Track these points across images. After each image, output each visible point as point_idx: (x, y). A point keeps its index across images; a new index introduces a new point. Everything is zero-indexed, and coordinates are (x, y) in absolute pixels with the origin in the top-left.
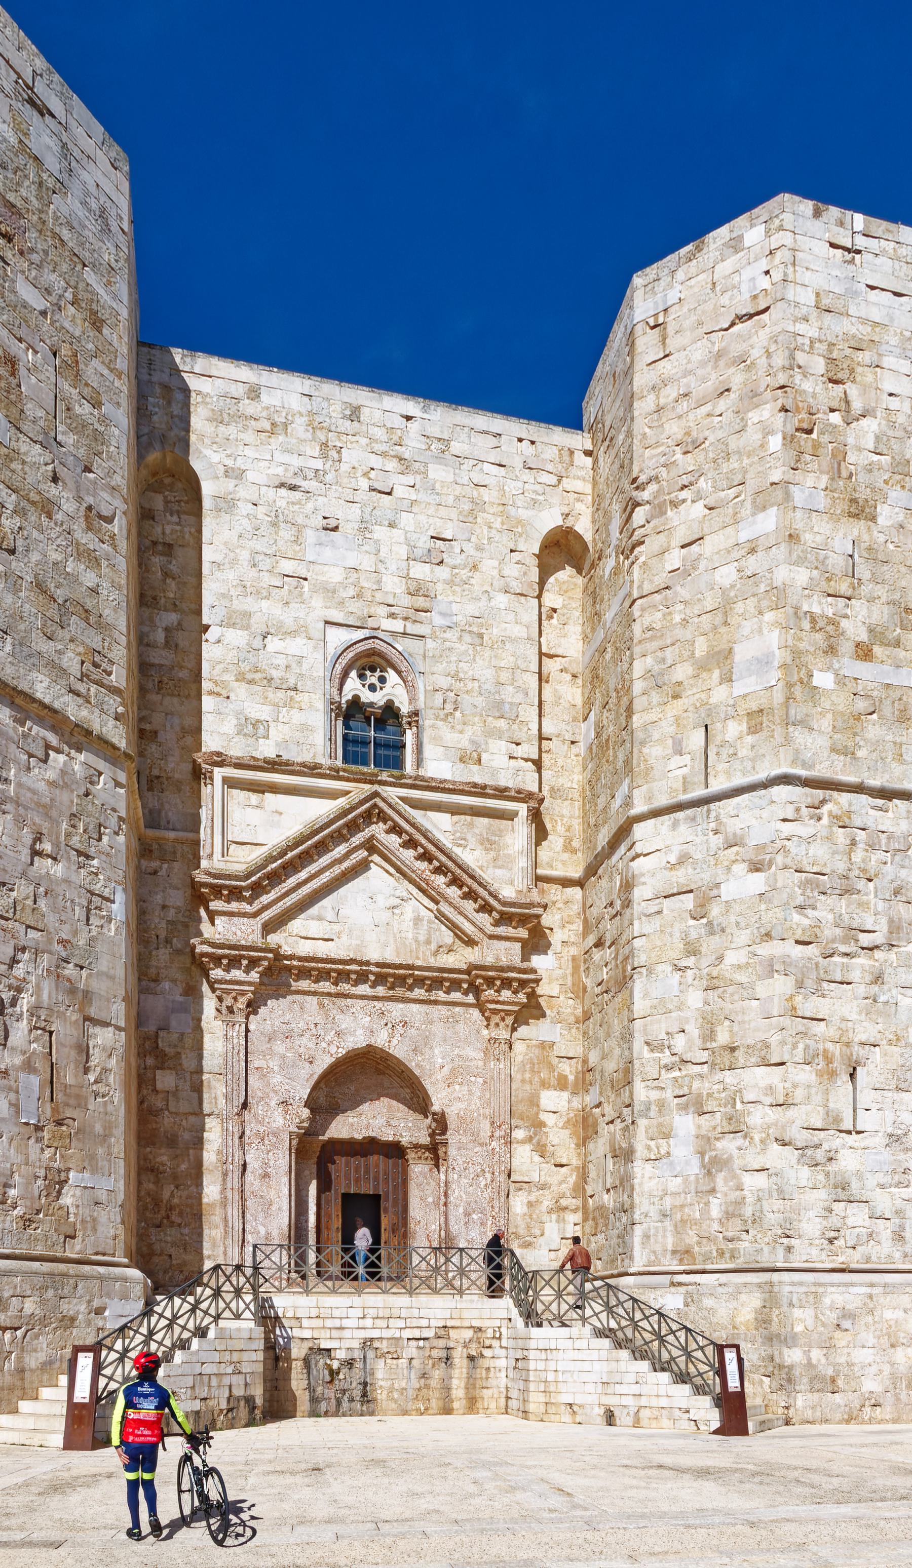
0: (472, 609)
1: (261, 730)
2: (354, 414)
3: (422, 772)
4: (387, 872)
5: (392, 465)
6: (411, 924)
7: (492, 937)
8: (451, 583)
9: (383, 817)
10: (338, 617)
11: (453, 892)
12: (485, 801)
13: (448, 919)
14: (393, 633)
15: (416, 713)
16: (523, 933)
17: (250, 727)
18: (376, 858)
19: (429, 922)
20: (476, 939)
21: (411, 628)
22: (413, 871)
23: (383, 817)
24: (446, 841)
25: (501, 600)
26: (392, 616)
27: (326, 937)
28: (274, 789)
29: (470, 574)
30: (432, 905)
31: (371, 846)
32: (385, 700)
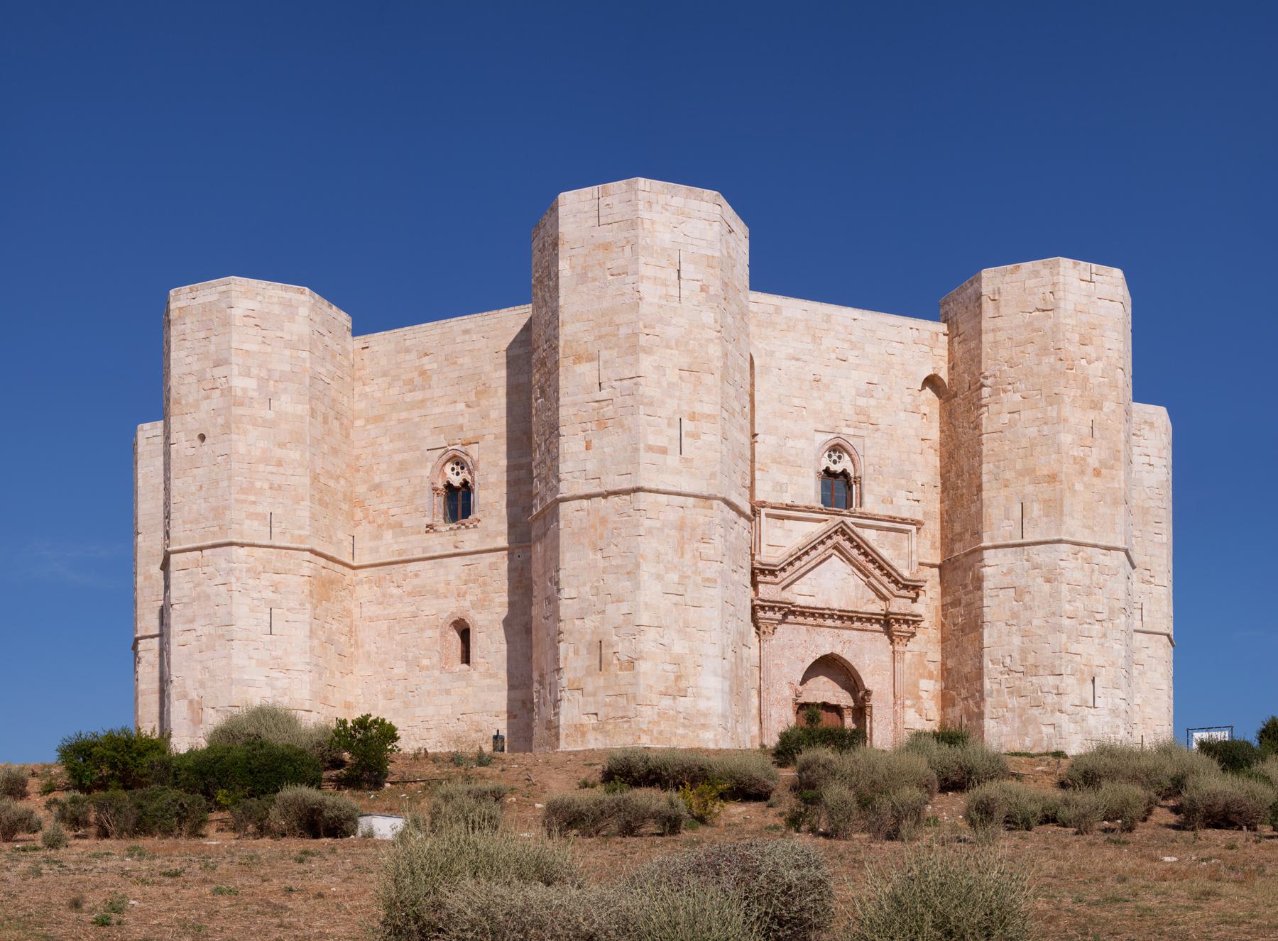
2: (828, 319)
3: (862, 510)
5: (846, 345)
12: (898, 525)
16: (912, 594)
21: (858, 432)
23: (844, 533)
24: (874, 545)
25: (902, 415)
26: (848, 426)
28: (789, 518)
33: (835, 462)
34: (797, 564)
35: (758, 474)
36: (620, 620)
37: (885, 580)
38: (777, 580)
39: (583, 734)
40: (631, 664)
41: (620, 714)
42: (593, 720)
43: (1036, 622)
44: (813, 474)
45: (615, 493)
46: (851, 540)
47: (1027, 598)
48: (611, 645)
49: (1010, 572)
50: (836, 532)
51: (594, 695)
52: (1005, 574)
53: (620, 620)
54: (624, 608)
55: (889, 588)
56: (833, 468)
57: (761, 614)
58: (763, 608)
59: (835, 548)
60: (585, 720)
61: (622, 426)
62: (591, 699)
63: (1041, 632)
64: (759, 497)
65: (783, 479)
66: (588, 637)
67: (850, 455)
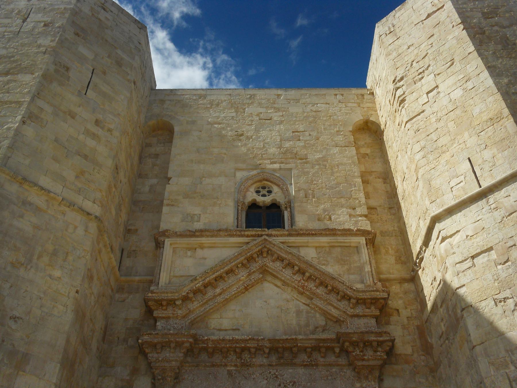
0: (318, 156)
1: (196, 218)
4: (276, 285)
6: (294, 315)
7: (353, 316)
8: (304, 147)
9: (269, 252)
10: (241, 166)
11: (321, 291)
13: (320, 308)
14: (274, 170)
15: (289, 202)
17: (189, 218)
18: (269, 278)
19: (308, 312)
20: (342, 319)
22: (293, 282)
27: (234, 328)
28: (202, 247)
29: (316, 142)
30: (308, 302)
31: (264, 271)
32: (271, 199)
33: (264, 195)
34: (210, 293)
35: (165, 209)
37: (333, 298)
38: (180, 312)
44: (231, 203)
46: (281, 259)
50: (260, 253)
55: (337, 308)
56: (260, 199)
57: (153, 356)
58: (154, 346)
59: (264, 271)
64: (163, 226)
65: (197, 211)
67: (278, 186)
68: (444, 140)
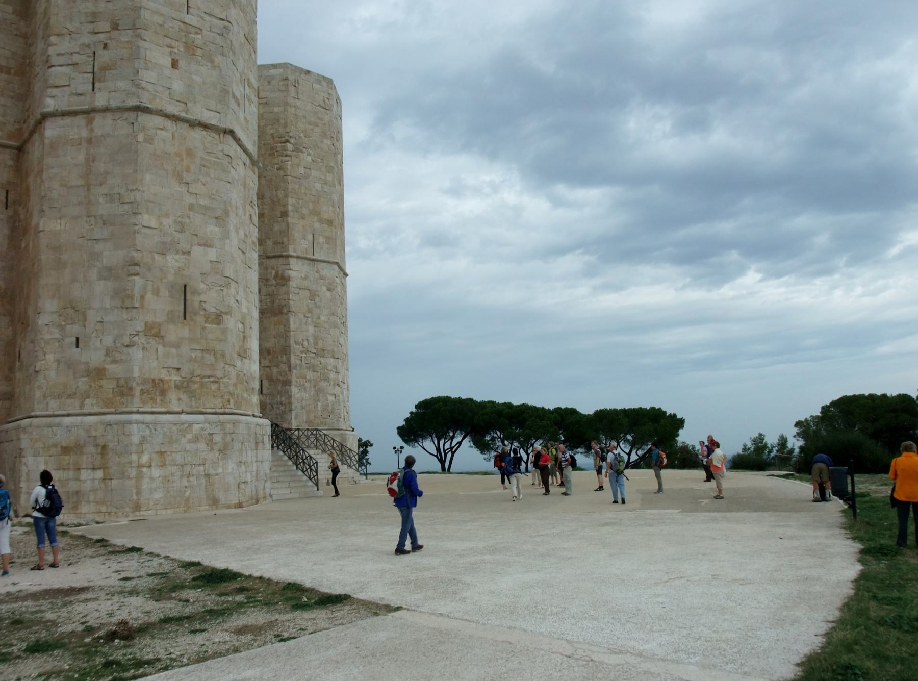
36: (207, 267)
39: (163, 392)
40: (218, 318)
41: (208, 373)
42: (175, 377)
43: (323, 318)
45: (205, 126)
47: (317, 300)
48: (196, 292)
49: (306, 278)
51: (177, 346)
52: (303, 279)
53: (207, 267)
54: (212, 254)
60: (164, 375)
61: (212, 62)
62: (174, 351)
63: (326, 326)
66: (171, 278)
68: (305, 211)
